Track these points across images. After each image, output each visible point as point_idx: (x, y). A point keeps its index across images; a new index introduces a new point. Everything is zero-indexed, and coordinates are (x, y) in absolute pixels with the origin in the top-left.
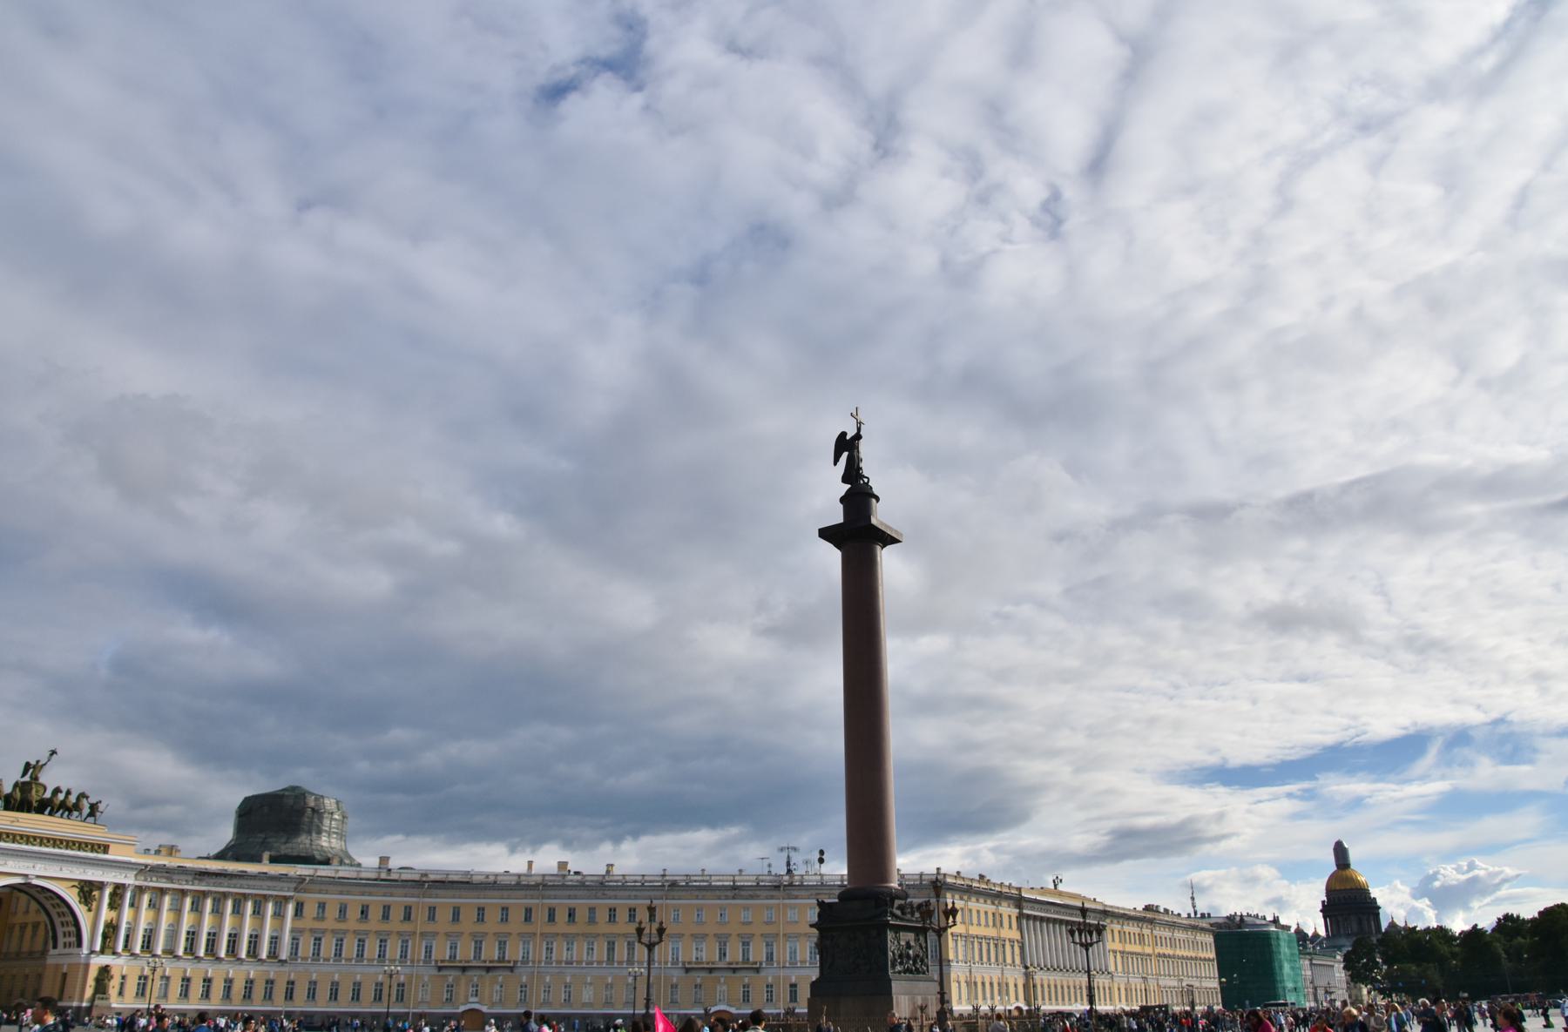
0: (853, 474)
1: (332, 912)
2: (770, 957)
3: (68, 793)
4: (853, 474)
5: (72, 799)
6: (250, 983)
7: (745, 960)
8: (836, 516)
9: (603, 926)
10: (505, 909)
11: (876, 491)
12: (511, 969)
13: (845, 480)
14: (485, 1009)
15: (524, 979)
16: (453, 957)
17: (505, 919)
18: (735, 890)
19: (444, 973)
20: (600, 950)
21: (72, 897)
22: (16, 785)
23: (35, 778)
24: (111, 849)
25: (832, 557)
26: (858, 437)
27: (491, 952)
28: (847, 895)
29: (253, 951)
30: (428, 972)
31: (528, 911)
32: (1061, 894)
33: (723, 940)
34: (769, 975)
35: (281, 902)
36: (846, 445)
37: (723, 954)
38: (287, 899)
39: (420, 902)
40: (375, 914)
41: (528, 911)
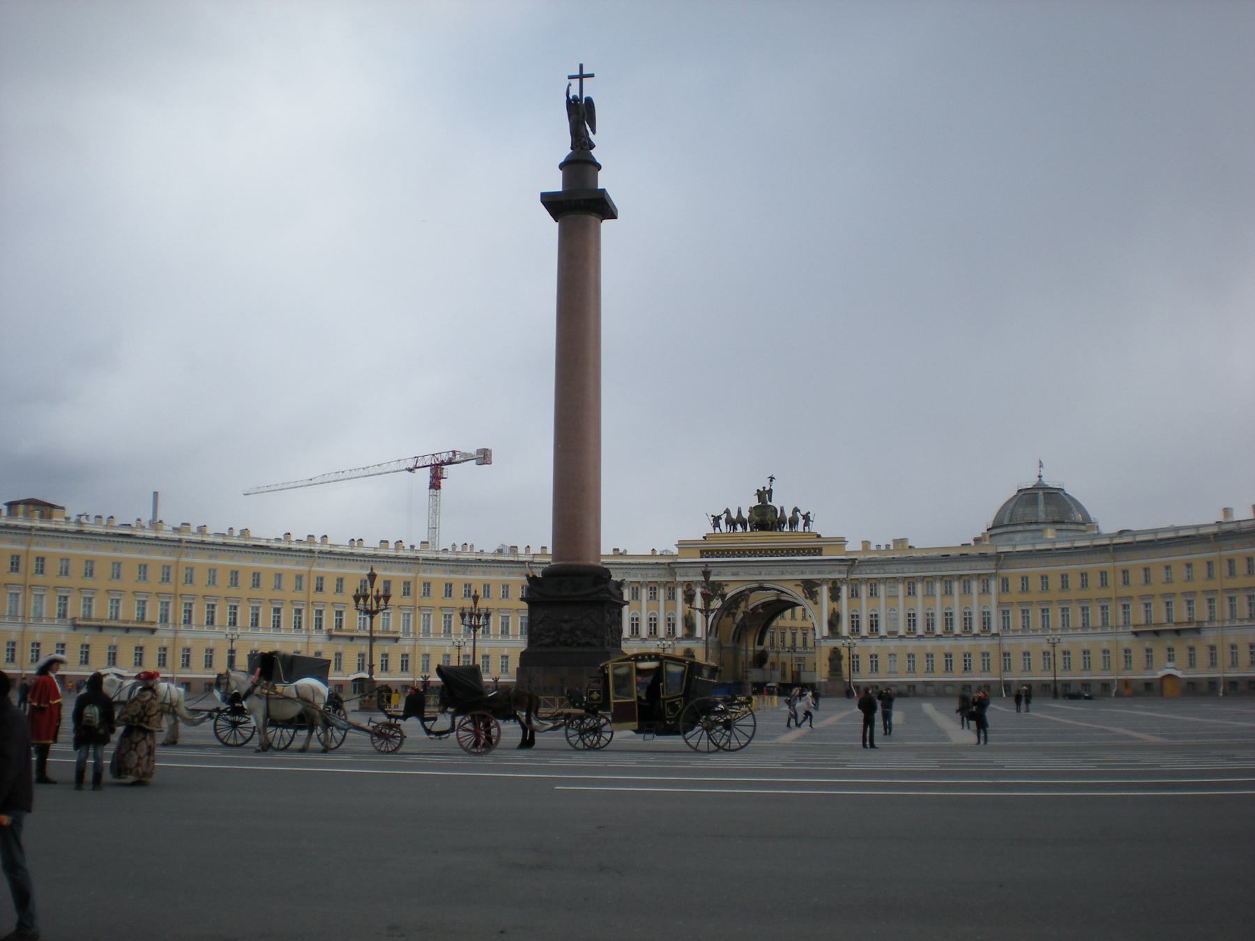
0: (581, 143)
1: (1035, 584)
3: (782, 511)
4: (581, 143)
5: (788, 515)
6: (967, 656)
14: (1179, 674)
21: (797, 594)
22: (753, 510)
23: (764, 502)
24: (824, 552)
27: (1181, 614)
28: (550, 574)
29: (967, 629)
30: (1127, 640)
35: (984, 579)
38: (990, 575)
39: (1112, 566)
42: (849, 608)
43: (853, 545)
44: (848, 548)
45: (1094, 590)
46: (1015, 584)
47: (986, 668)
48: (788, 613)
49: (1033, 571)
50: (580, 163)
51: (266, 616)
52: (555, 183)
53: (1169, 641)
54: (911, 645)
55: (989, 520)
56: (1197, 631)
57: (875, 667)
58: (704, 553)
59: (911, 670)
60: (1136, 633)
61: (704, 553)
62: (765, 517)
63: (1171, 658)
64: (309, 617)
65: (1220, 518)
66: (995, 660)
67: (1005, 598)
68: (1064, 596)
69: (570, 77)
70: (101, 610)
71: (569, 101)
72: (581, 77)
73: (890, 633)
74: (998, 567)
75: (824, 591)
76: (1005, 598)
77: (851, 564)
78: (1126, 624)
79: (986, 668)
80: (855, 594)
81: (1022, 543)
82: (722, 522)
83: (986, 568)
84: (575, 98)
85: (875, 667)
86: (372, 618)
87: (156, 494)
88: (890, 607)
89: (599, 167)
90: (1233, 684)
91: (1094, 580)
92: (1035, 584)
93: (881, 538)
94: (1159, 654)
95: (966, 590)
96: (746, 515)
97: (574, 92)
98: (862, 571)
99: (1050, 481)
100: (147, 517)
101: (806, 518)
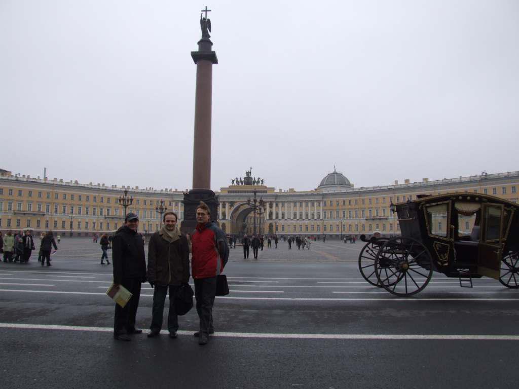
0: (206, 35)
4: (206, 35)
5: (257, 180)
14: (380, 232)
19: (368, 221)
22: (245, 178)
29: (313, 217)
30: (363, 222)
38: (321, 201)
40: (347, 203)
42: (276, 210)
43: (277, 190)
44: (275, 191)
45: (353, 205)
46: (328, 203)
47: (318, 230)
48: (253, 212)
49: (334, 199)
51: (83, 210)
52: (196, 49)
53: (377, 222)
54: (295, 222)
55: (319, 184)
57: (283, 229)
58: (229, 192)
59: (295, 230)
60: (367, 220)
61: (229, 192)
62: (249, 180)
63: (377, 228)
64: (98, 211)
66: (321, 227)
67: (325, 208)
69: (202, 11)
70: (24, 208)
71: (201, 20)
72: (206, 11)
73: (289, 219)
74: (323, 198)
75: (268, 205)
76: (325, 208)
77: (277, 196)
78: (363, 216)
79: (318, 230)
80: (277, 205)
81: (331, 190)
82: (235, 182)
83: (319, 198)
84: (204, 18)
85: (283, 229)
86: (126, 208)
87: (45, 169)
88: (288, 210)
89: (212, 44)
91: (353, 202)
92: (335, 204)
93: (286, 188)
94: (374, 226)
95: (313, 205)
96: (243, 180)
97: (204, 16)
98: (294, 198)
99: (338, 171)
100: (42, 178)
101: (262, 181)
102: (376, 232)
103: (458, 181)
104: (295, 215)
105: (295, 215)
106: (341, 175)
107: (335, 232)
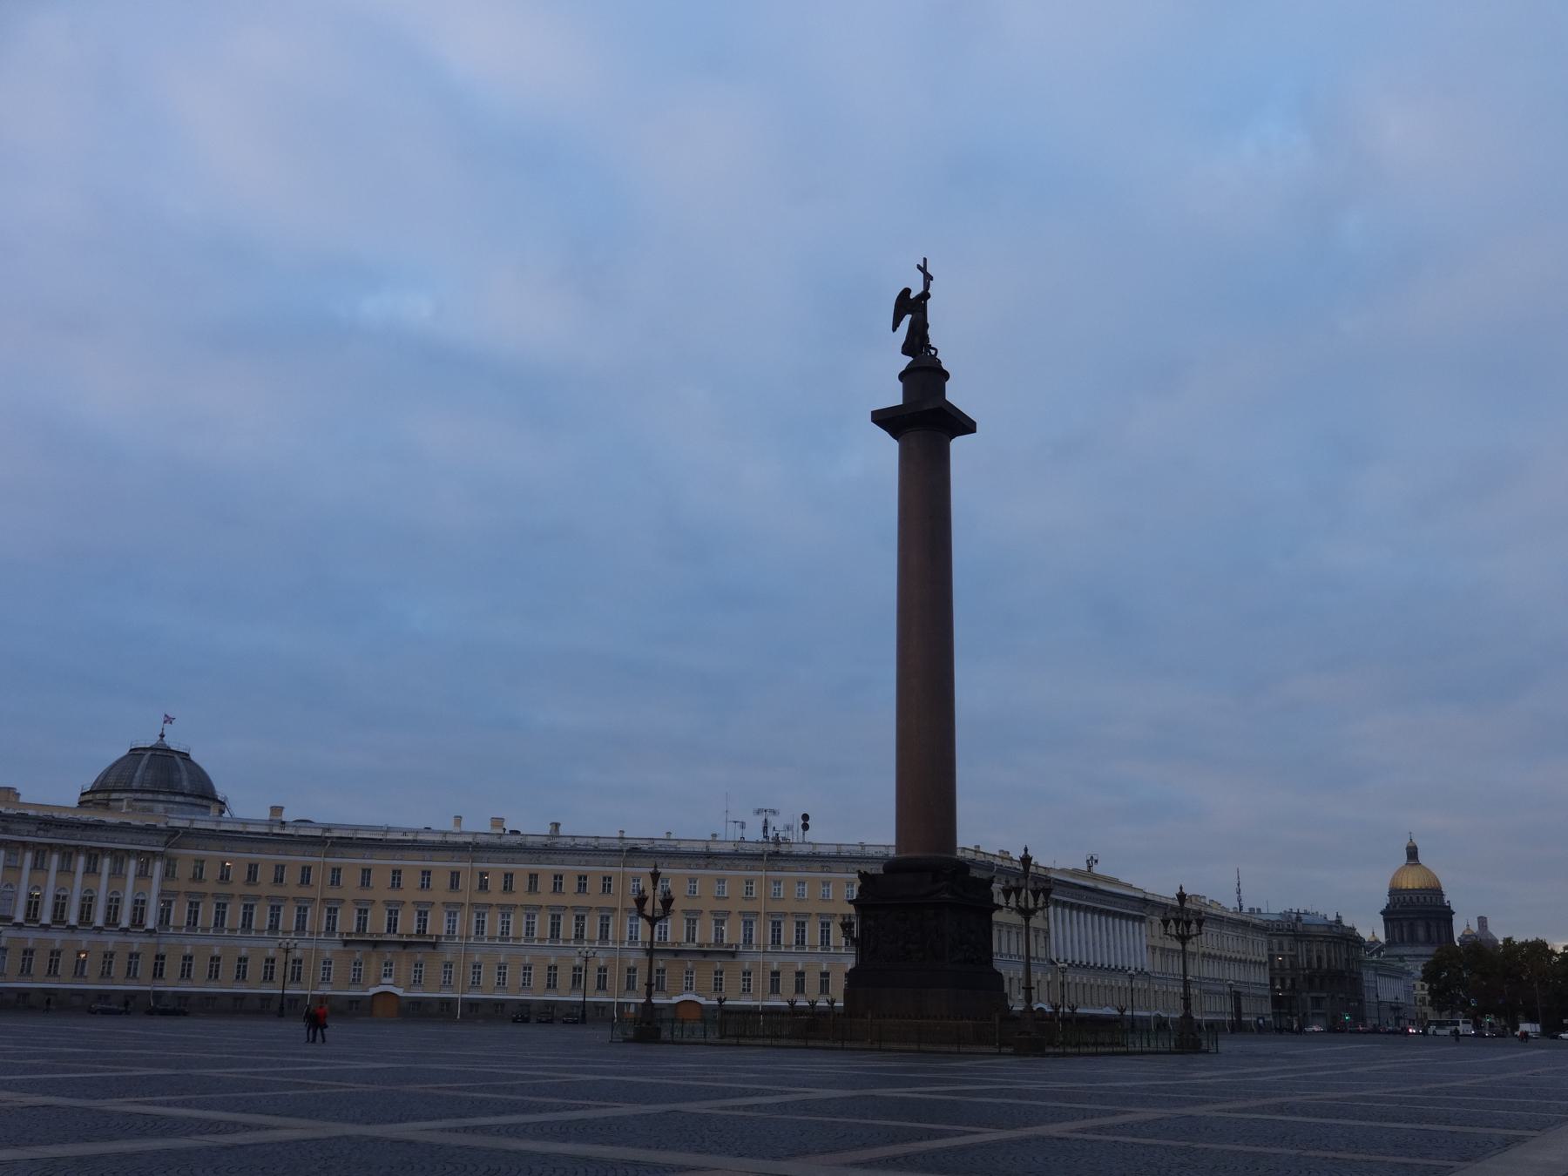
0: (917, 343)
2: (748, 940)
4: (917, 343)
7: (719, 941)
8: (893, 395)
9: (545, 896)
10: (426, 873)
11: (945, 366)
12: (434, 945)
13: (906, 350)
14: (400, 992)
15: (449, 958)
16: (361, 928)
17: (425, 885)
18: (708, 857)
20: (542, 924)
25: (886, 450)
26: (925, 295)
27: (408, 924)
28: (893, 867)
30: (331, 948)
31: (455, 876)
32: (1096, 877)
33: (692, 918)
34: (746, 962)
35: (146, 858)
36: (911, 307)
37: (691, 938)
41: (455, 876)
50: (924, 371)
54: (31, 937)
56: (733, 954)
60: (346, 943)
65: (449, 826)
68: (251, 891)
76: (172, 886)
78: (331, 929)
90: (472, 1006)
92: (211, 872)
99: (173, 742)
102: (381, 989)
103: (700, 847)
104: (33, 906)
105: (33, 906)
106: (185, 756)
107: (226, 986)
